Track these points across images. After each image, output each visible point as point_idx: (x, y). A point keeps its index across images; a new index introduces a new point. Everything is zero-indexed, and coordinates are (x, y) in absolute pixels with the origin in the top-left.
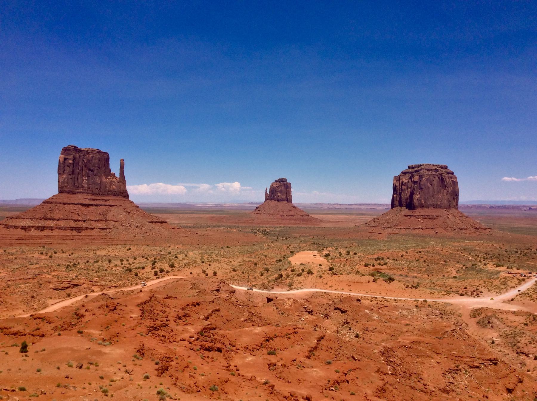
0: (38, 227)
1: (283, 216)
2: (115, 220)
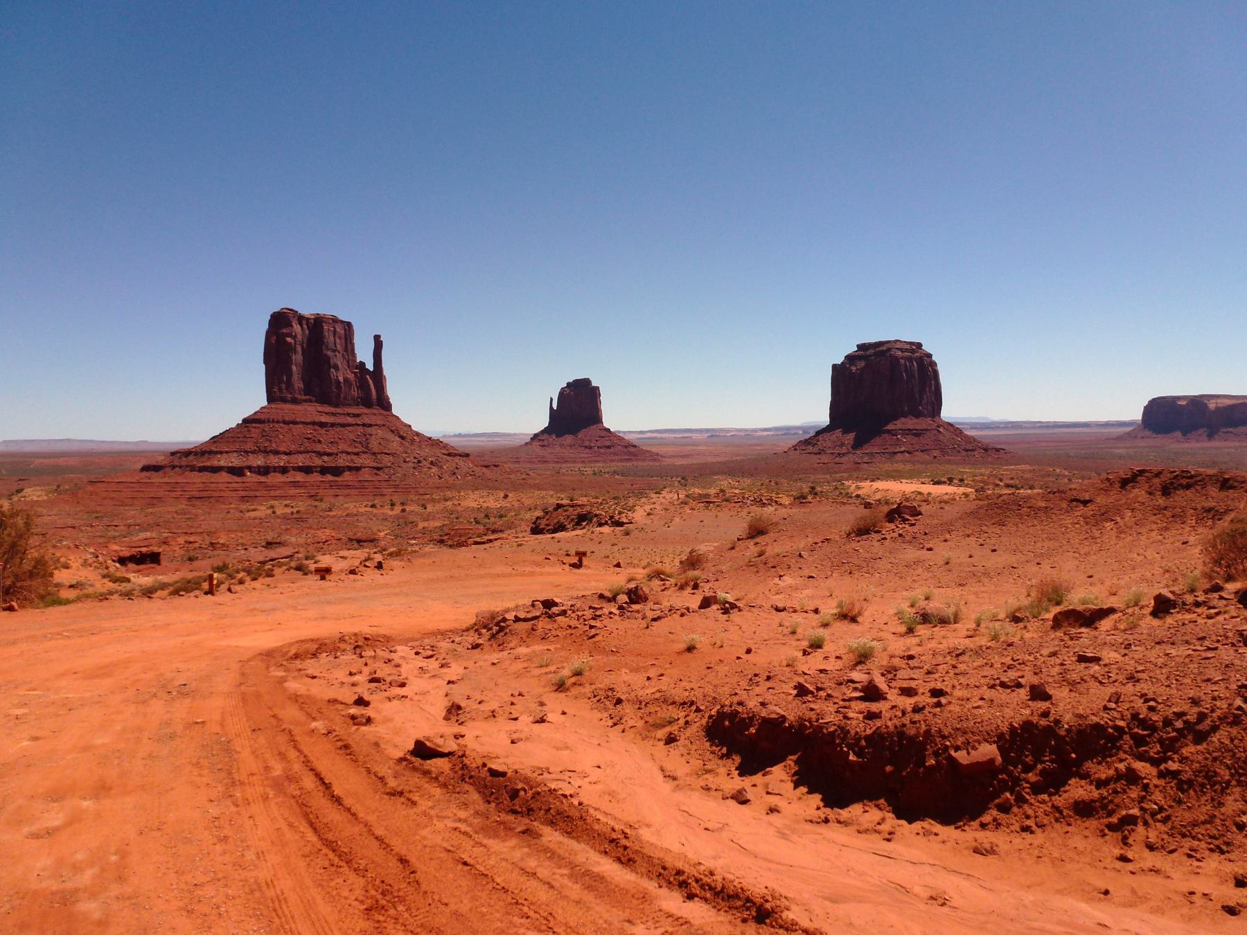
0: (259, 467)
1: (591, 448)
2: (387, 451)
